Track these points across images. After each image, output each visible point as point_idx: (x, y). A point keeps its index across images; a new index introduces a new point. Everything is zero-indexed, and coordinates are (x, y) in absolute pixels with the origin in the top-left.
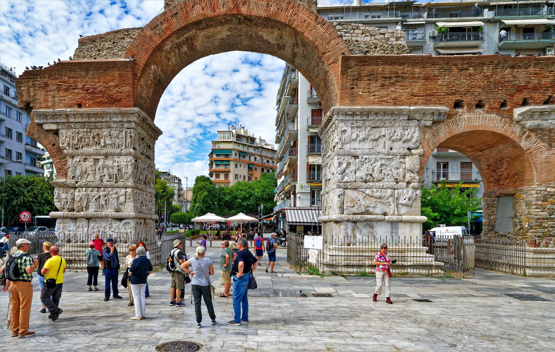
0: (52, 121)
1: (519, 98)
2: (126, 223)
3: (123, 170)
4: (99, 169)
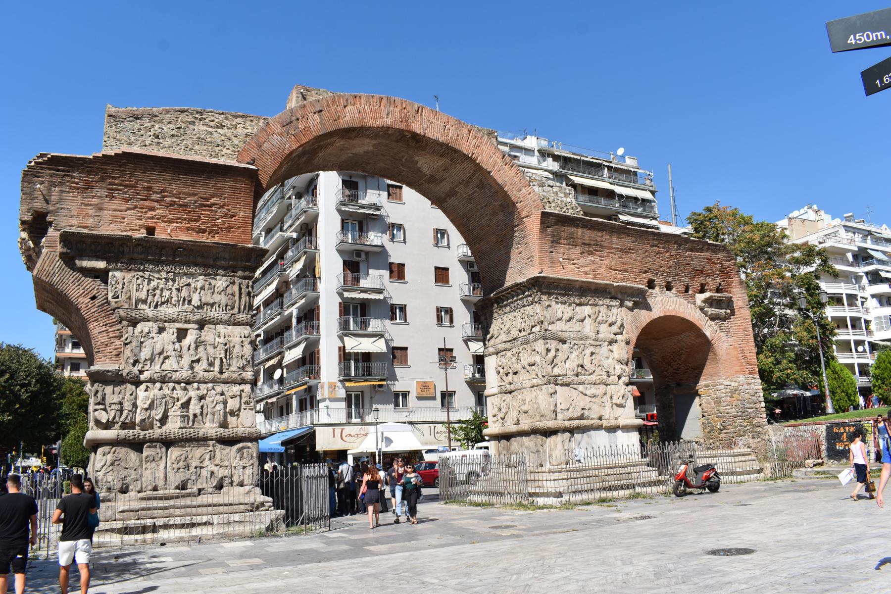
2: (243, 448)
4: (189, 349)
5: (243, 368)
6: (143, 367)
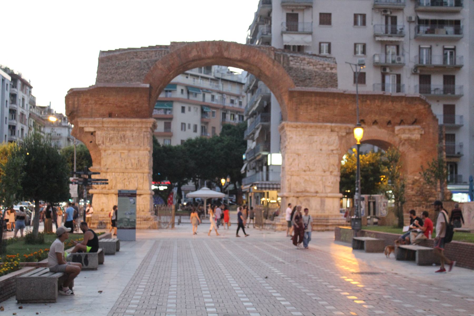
0: (92, 126)
1: (398, 120)
3: (142, 161)
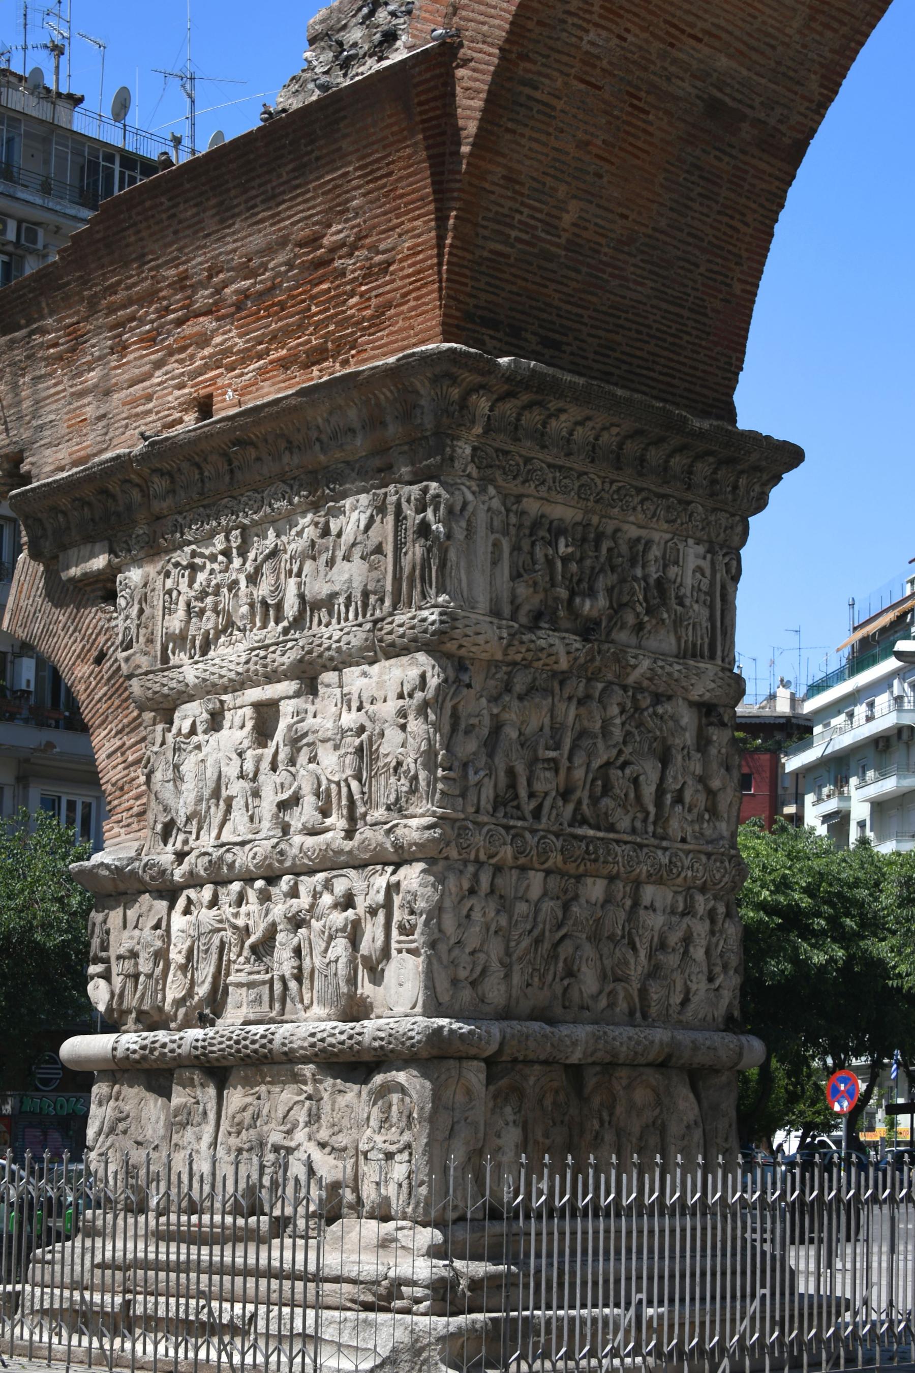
4: (274, 768)
5: (397, 807)
6: (186, 842)
